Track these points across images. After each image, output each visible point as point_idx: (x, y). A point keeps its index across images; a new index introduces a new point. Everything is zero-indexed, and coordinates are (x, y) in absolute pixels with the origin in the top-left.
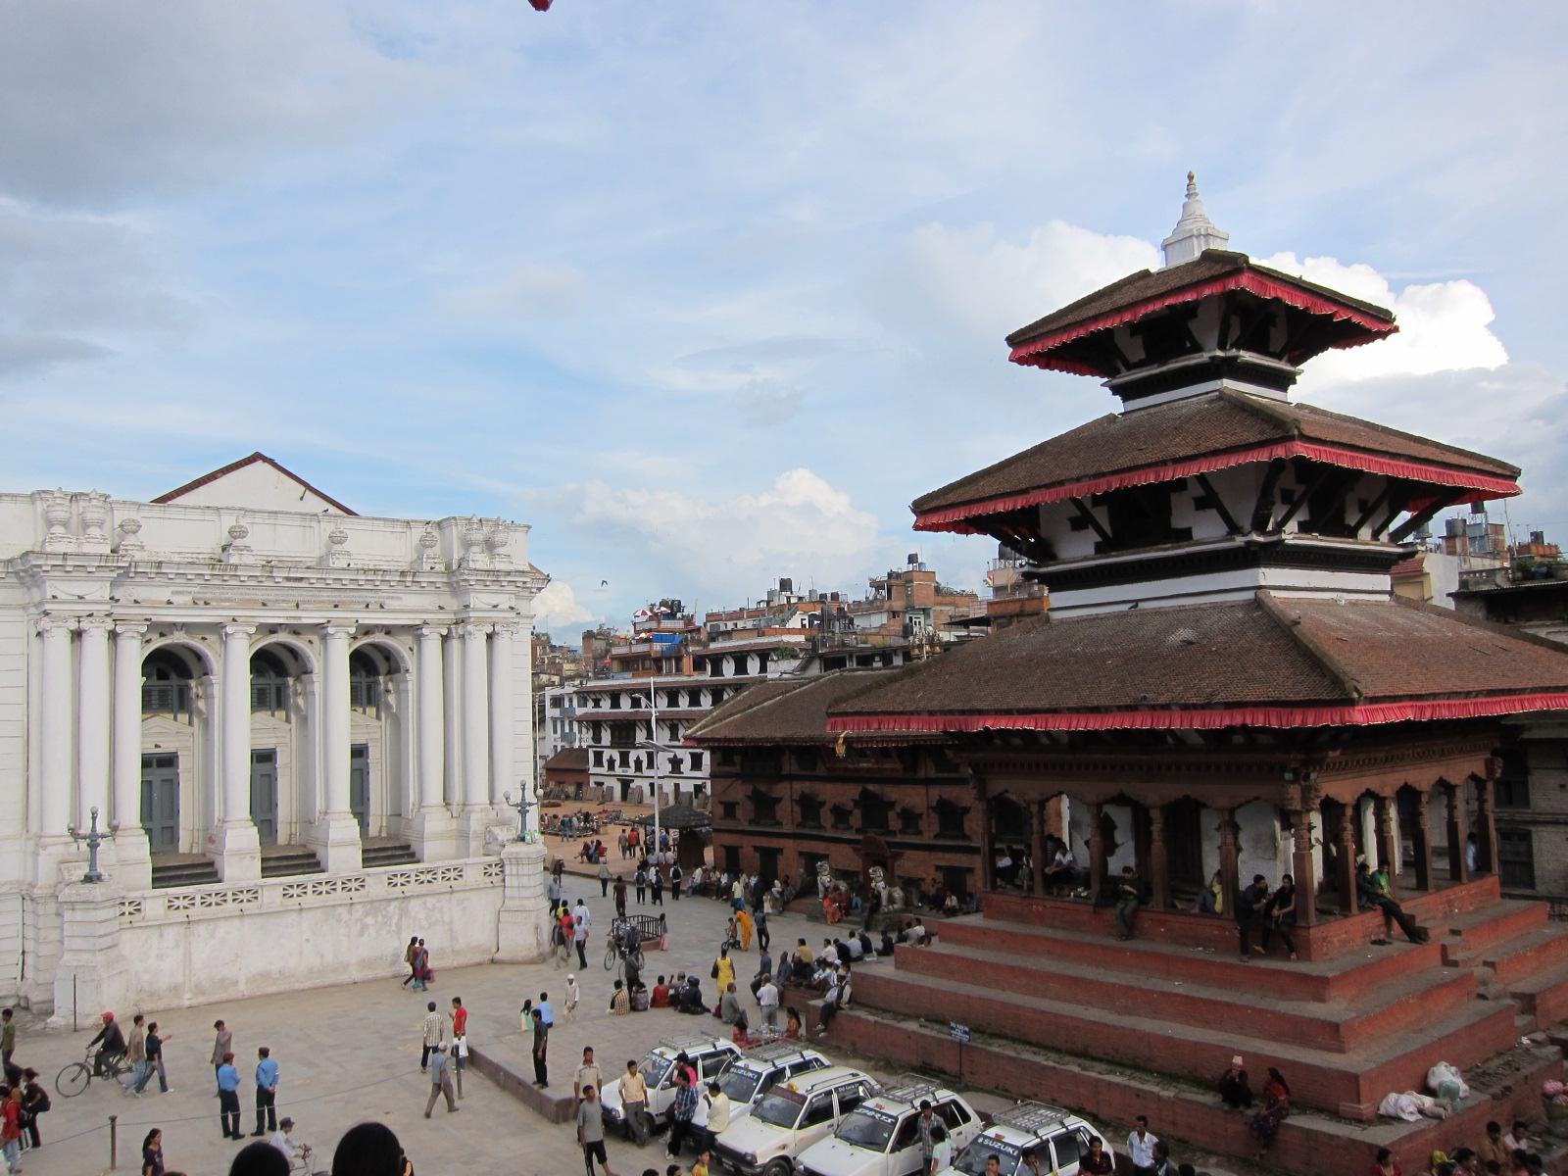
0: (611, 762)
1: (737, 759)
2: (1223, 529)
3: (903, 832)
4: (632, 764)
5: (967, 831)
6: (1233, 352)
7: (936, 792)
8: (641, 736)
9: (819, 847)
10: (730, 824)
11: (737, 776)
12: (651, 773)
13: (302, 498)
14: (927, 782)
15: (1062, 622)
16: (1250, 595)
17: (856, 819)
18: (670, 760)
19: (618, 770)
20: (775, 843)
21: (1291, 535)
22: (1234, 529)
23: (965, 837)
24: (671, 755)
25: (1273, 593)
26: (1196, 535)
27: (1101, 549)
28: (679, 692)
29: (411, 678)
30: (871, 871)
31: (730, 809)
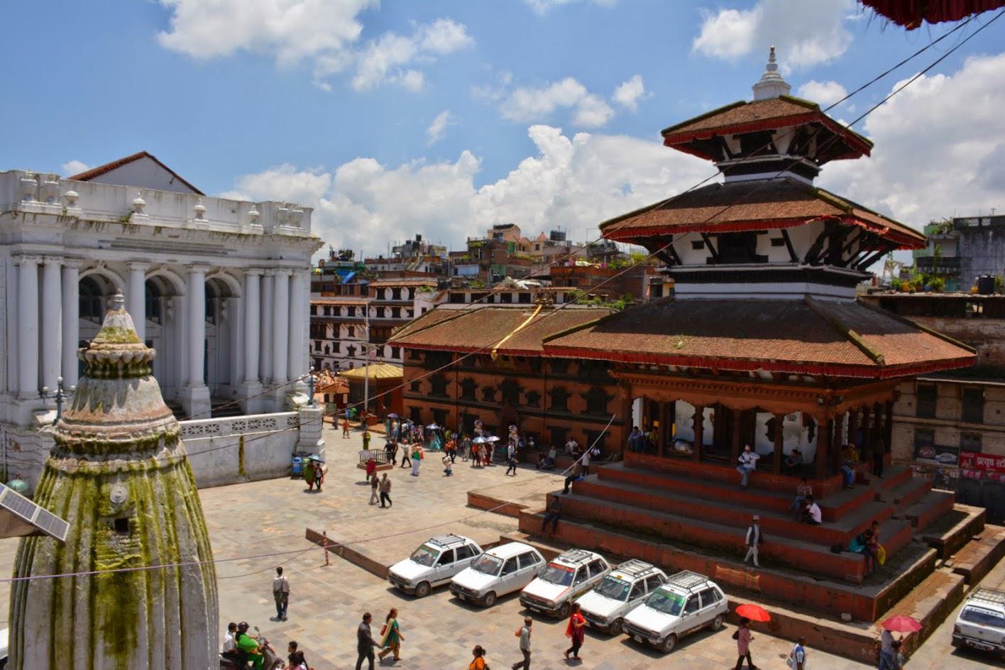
0: (327, 349)
1: (422, 356)
2: (789, 258)
3: (528, 405)
4: (323, 349)
5: (569, 407)
6: (797, 158)
7: (551, 384)
8: (330, 333)
9: (473, 411)
10: (415, 394)
11: (421, 366)
12: (336, 355)
13: (171, 183)
14: (546, 377)
15: (683, 301)
16: (802, 297)
17: (498, 396)
18: (348, 348)
19: (314, 352)
20: (445, 407)
21: (826, 268)
22: (794, 259)
23: (566, 410)
24: (349, 345)
25: (814, 297)
26: (771, 259)
27: (709, 261)
28: (340, 307)
29: (239, 301)
30: (510, 427)
31: (415, 386)
